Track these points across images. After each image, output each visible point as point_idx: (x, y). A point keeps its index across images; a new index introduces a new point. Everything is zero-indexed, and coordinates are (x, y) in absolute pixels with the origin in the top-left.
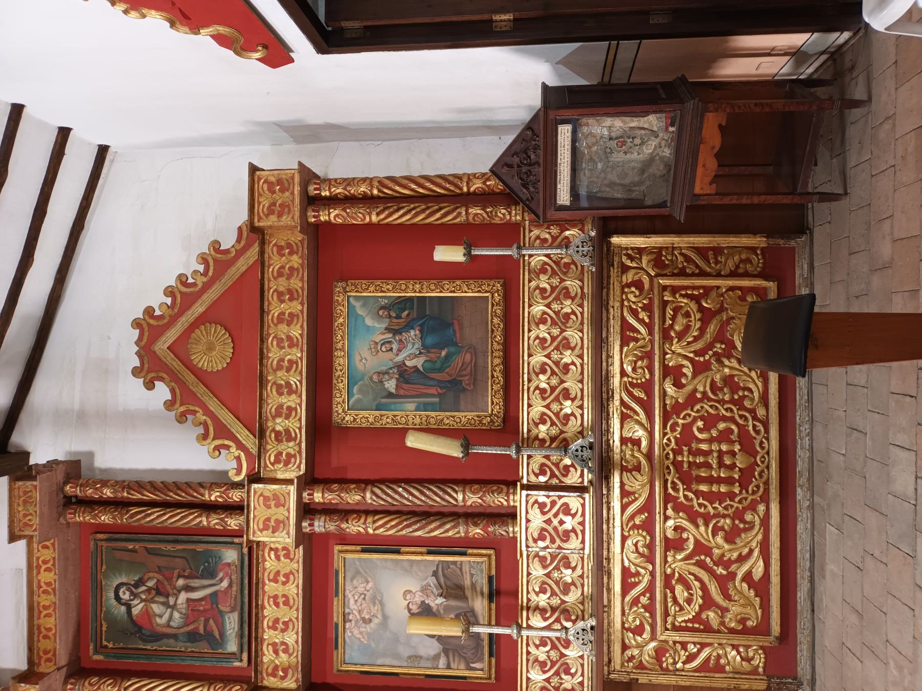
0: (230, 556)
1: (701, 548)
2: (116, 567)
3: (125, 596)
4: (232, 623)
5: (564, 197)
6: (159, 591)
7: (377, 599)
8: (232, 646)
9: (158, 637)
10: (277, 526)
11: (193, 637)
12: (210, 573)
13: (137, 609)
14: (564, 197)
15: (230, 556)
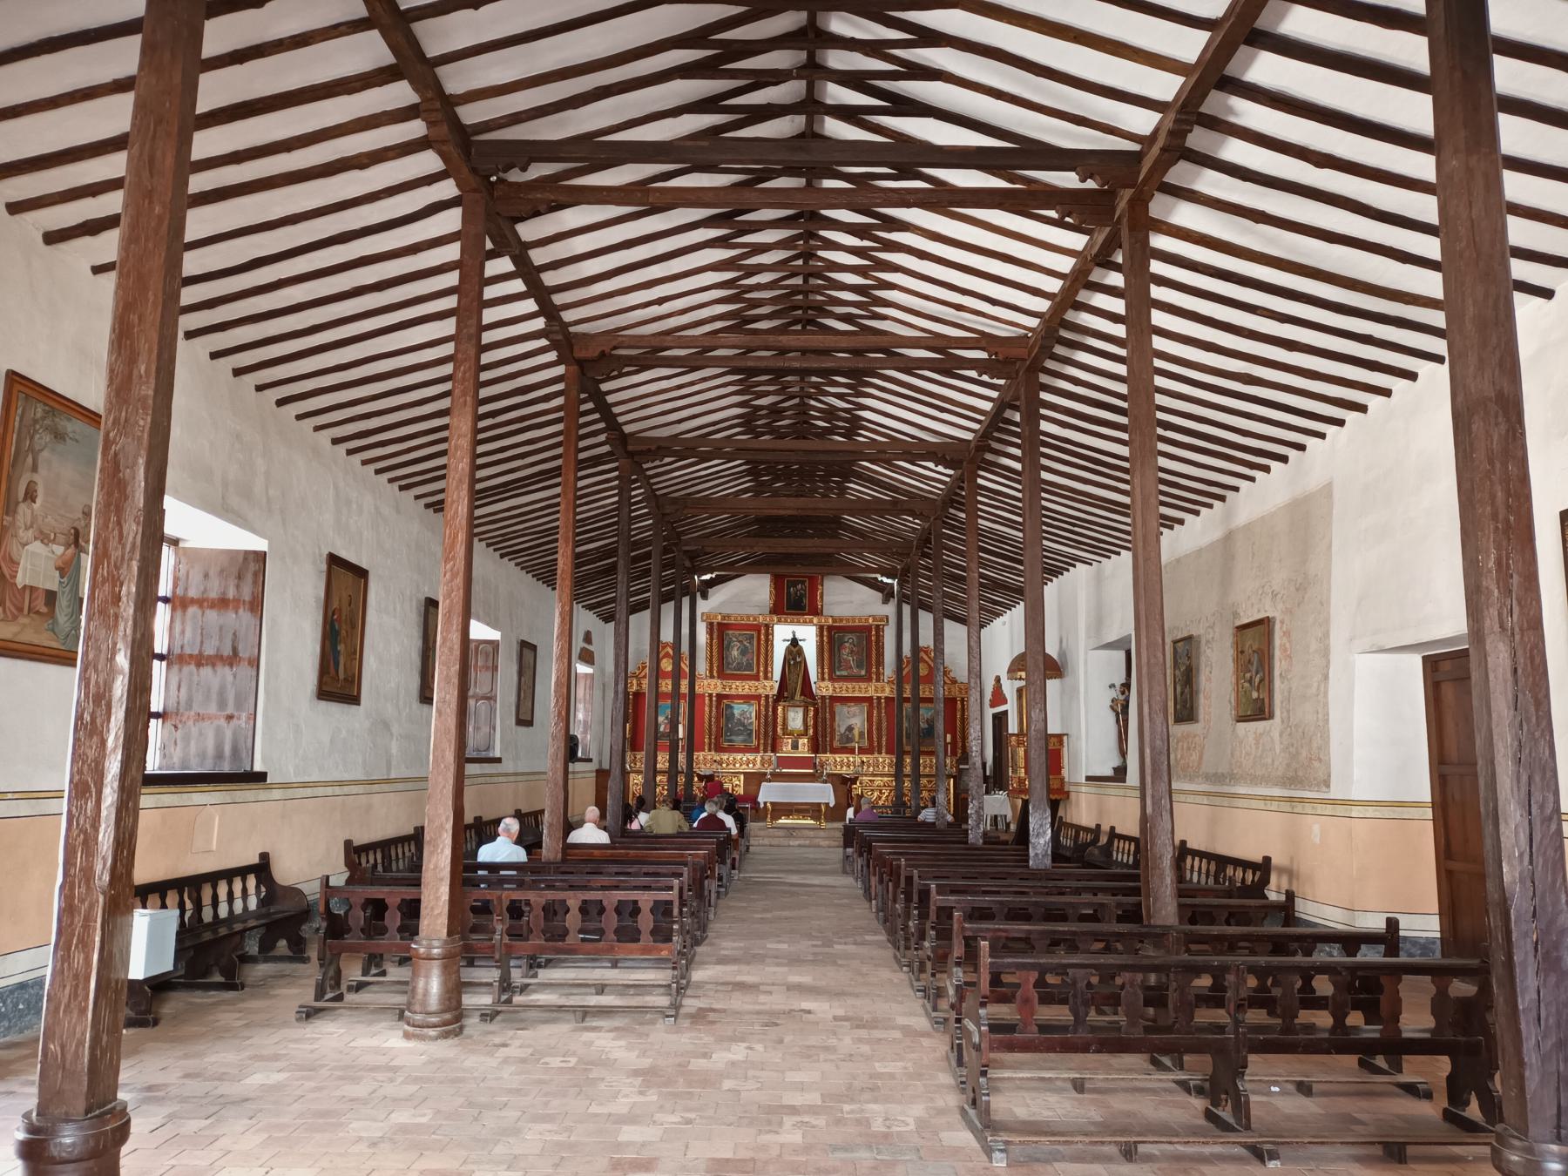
0: (863, 673)
1: (880, 798)
2: (858, 638)
3: (851, 641)
4: (844, 673)
5: (961, 767)
6: (852, 651)
7: (854, 716)
8: (838, 673)
9: (839, 651)
10: (876, 691)
11: (840, 662)
12: (858, 667)
13: (847, 645)
14: (961, 767)
15: (863, 673)
